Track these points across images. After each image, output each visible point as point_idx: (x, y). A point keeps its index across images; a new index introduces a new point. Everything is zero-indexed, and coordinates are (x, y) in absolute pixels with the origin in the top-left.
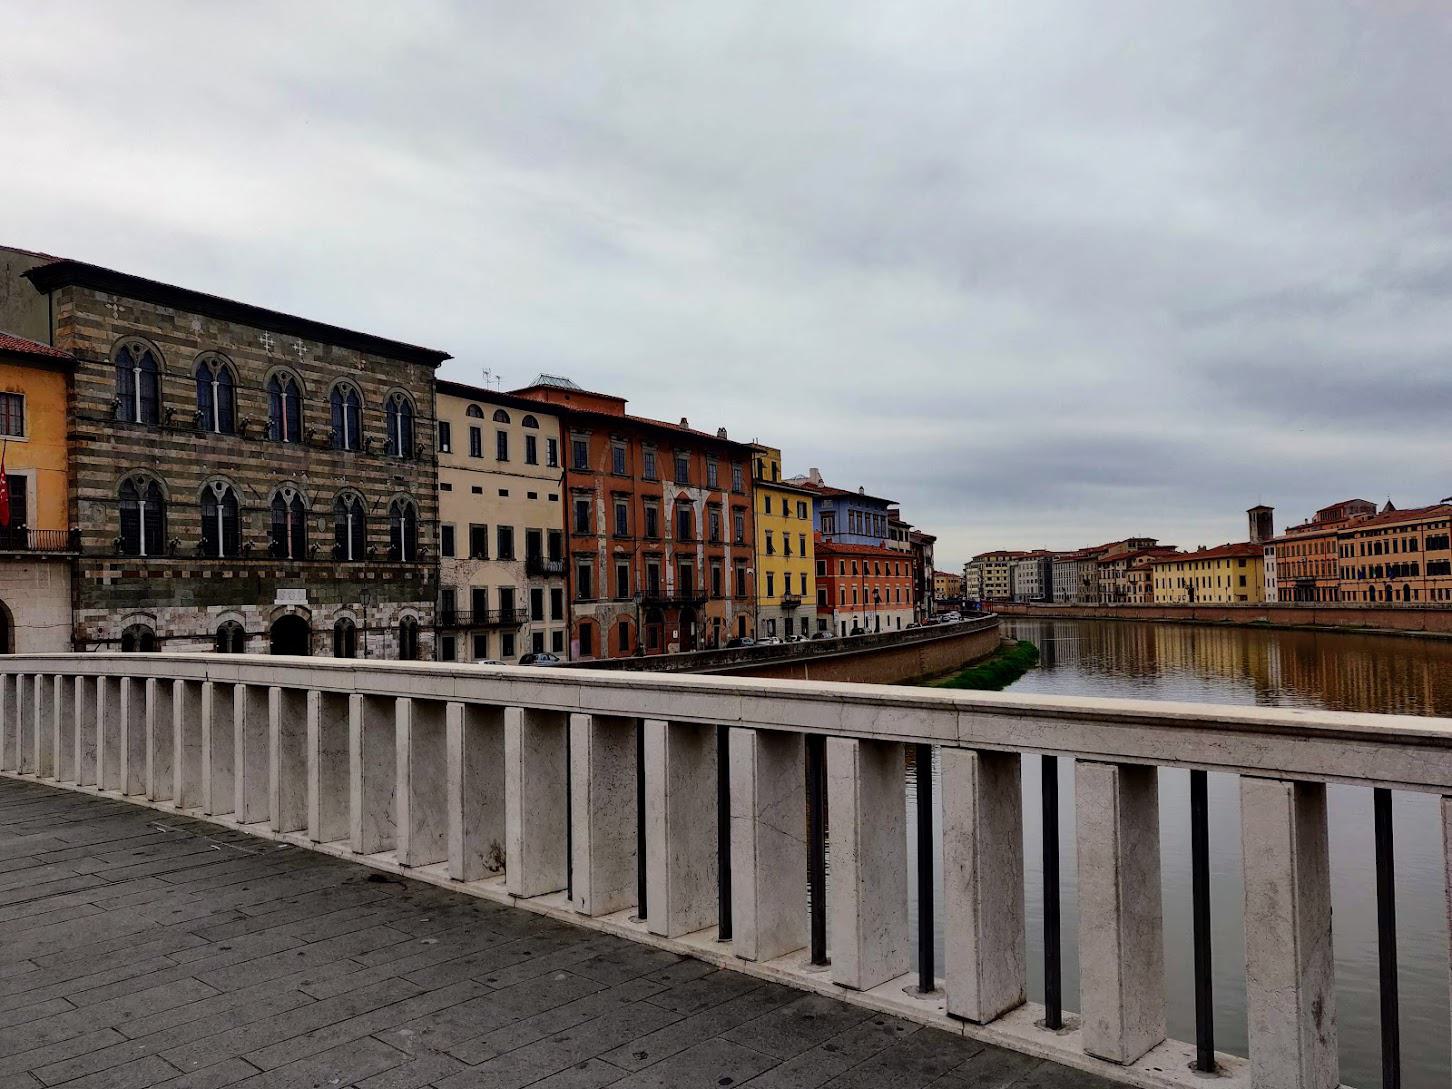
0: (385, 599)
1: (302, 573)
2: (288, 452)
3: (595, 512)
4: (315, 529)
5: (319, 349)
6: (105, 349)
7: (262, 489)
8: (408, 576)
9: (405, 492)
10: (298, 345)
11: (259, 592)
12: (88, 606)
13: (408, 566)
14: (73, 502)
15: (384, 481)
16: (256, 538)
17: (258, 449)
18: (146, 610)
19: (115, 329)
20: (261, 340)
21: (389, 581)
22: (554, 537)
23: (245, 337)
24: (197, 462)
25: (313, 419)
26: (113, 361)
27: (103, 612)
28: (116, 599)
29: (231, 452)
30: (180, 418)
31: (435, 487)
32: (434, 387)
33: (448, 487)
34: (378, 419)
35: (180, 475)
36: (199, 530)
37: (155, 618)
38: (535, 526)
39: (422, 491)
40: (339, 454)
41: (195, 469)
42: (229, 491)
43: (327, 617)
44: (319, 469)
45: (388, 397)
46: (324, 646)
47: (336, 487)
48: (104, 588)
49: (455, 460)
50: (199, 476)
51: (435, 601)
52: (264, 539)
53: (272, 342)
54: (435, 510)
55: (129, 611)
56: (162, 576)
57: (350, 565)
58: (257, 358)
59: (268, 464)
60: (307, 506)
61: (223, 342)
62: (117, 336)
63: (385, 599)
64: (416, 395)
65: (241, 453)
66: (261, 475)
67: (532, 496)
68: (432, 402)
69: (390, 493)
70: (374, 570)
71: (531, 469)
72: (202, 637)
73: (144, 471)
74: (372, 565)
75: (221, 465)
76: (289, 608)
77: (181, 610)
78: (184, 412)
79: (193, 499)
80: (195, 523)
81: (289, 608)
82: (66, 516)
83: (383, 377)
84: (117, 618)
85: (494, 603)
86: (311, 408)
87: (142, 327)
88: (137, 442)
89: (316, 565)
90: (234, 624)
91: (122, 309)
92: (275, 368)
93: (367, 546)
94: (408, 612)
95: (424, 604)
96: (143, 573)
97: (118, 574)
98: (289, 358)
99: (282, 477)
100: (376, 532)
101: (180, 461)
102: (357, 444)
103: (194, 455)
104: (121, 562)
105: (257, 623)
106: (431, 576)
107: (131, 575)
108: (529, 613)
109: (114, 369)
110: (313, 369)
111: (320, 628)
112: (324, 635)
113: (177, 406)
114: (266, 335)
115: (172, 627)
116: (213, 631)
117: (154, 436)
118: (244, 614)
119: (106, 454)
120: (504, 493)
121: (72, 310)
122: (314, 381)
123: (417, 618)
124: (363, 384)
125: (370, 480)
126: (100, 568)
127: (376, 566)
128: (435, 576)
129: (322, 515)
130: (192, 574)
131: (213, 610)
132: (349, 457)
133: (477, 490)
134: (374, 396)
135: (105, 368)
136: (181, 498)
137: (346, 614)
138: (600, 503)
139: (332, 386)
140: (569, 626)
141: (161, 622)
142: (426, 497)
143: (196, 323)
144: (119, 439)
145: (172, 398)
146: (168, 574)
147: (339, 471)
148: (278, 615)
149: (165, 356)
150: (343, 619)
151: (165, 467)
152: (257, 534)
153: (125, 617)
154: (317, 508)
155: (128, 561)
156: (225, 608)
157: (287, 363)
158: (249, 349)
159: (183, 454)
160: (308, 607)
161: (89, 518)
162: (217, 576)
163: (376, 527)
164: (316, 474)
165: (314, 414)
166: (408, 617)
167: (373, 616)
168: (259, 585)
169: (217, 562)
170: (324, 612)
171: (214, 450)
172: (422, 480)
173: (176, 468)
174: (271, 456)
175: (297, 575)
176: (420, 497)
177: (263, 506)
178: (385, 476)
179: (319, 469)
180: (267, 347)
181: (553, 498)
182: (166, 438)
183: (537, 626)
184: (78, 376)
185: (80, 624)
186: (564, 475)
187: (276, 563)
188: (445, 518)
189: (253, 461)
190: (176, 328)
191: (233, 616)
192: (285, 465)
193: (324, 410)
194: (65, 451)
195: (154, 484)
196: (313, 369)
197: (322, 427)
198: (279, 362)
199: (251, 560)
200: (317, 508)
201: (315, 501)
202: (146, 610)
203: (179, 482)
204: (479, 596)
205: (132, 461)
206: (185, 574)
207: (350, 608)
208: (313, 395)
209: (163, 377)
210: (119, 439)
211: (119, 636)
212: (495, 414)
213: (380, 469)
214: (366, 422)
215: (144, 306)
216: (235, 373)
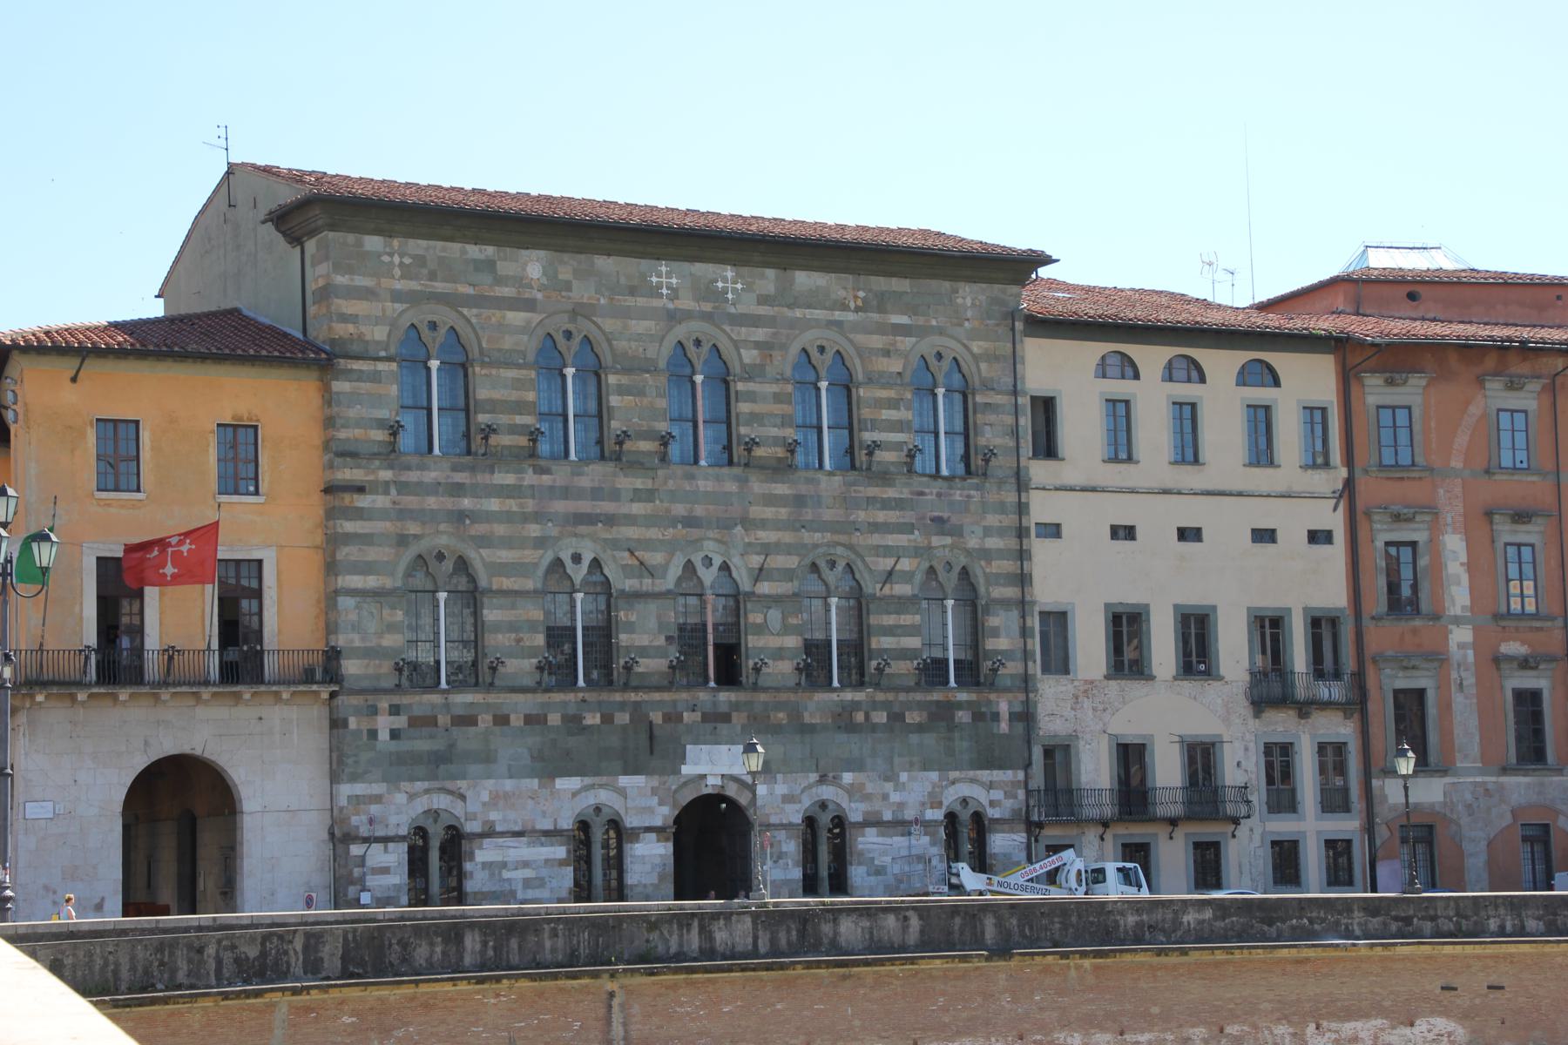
0: (912, 764)
1: (734, 715)
2: (704, 485)
3: (1437, 566)
4: (761, 629)
5: (769, 279)
6: (379, 333)
7: (655, 558)
8: (963, 716)
9: (952, 547)
10: (725, 280)
11: (652, 753)
12: (354, 778)
13: (963, 696)
14: (331, 598)
15: (907, 528)
16: (644, 651)
17: (649, 484)
18: (449, 785)
19: (397, 296)
20: (654, 279)
21: (920, 728)
22: (1319, 624)
23: (623, 280)
24: (538, 517)
25: (755, 418)
26: (393, 351)
27: (378, 788)
28: (401, 766)
29: (596, 494)
30: (505, 440)
31: (1022, 532)
32: (1019, 325)
33: (1053, 531)
34: (893, 404)
35: (508, 543)
36: (540, 640)
37: (463, 797)
38: (1270, 602)
39: (993, 543)
40: (809, 481)
41: (534, 530)
42: (596, 564)
43: (788, 799)
44: (769, 513)
45: (915, 360)
46: (780, 856)
47: (804, 546)
48: (379, 746)
50: (541, 543)
51: (1028, 766)
52: (659, 652)
53: (674, 281)
54: (1023, 580)
55: (420, 786)
56: (476, 724)
57: (834, 696)
58: (644, 314)
59: (668, 510)
60: (746, 586)
61: (583, 292)
62: (399, 307)
63: (912, 764)
64: (977, 347)
65: (615, 495)
66: (653, 533)
67: (1264, 536)
68: (1015, 359)
69: (917, 552)
70: (886, 705)
72: (546, 833)
73: (443, 541)
74: (880, 696)
76: (711, 781)
77: (509, 785)
78: (514, 429)
79: (530, 585)
80: (532, 626)
81: (711, 781)
82: (322, 624)
83: (903, 319)
84: (400, 798)
85: (1167, 772)
86: (751, 397)
87: (440, 286)
88: (434, 488)
89: (763, 697)
90: (605, 810)
91: (407, 261)
92: (680, 332)
93: (870, 659)
94: (965, 790)
95: (1007, 775)
96: (443, 720)
97: (401, 722)
98: (707, 307)
99: (695, 533)
100: (890, 631)
101: (507, 517)
102: (854, 458)
103: (530, 505)
104: (405, 700)
105: (650, 810)
106: (1013, 717)
107: (423, 722)
108: (1258, 797)
109: (394, 366)
110: (754, 321)
111: (774, 820)
112: (782, 835)
113: (504, 419)
114: (664, 269)
115: (494, 816)
116: (567, 823)
117: (460, 477)
118: (622, 792)
119: (383, 515)
120: (1188, 534)
121: (328, 275)
122: (757, 345)
123: (985, 803)
124: (860, 338)
125: (875, 527)
126: (373, 711)
127: (890, 696)
128: (1026, 717)
129: (776, 600)
130: (529, 720)
131: (566, 784)
132: (831, 485)
133: (1123, 533)
134: (885, 360)
135: (381, 366)
136: (507, 583)
137: (827, 792)
138: (1454, 545)
139: (795, 349)
140: (1369, 828)
141: (473, 806)
142: (1001, 554)
143: (533, 265)
144: (403, 487)
145: (493, 406)
146: (485, 720)
147: (808, 514)
148: (687, 796)
149: (480, 332)
150: (823, 805)
151: (480, 529)
152: (646, 643)
153: (412, 797)
154: (765, 588)
155: (417, 698)
156: (588, 780)
157: (707, 317)
158: (630, 301)
159: (512, 505)
161: (356, 627)
162: (573, 722)
163: (889, 620)
164: (763, 524)
165: (758, 408)
166: (965, 801)
167: (885, 797)
168: (651, 737)
169: (570, 697)
170: (781, 789)
171: (566, 493)
172: (992, 520)
173: (500, 530)
174: (674, 497)
176: (986, 554)
177: (657, 589)
178: (909, 516)
179: (769, 513)
180: (665, 291)
181: (1318, 537)
182: (483, 478)
183: (1283, 826)
184: (339, 386)
185: (341, 809)
186: (1349, 483)
187: (684, 695)
188: (1046, 594)
189: (637, 508)
190: (500, 281)
191: (604, 797)
192: (699, 511)
193: (778, 398)
194: (321, 512)
195: (462, 565)
196: (754, 321)
197: (774, 432)
198: (688, 315)
199: (636, 689)
200: (765, 588)
201: (760, 574)
202: (449, 785)
203: (505, 555)
204: (1131, 756)
205: (424, 523)
206: (516, 721)
207: (836, 781)
208: (751, 374)
209: (477, 369)
210: (403, 487)
211: (403, 831)
212: (1170, 366)
213: (899, 504)
214: (866, 413)
215: (444, 249)
216: (605, 345)
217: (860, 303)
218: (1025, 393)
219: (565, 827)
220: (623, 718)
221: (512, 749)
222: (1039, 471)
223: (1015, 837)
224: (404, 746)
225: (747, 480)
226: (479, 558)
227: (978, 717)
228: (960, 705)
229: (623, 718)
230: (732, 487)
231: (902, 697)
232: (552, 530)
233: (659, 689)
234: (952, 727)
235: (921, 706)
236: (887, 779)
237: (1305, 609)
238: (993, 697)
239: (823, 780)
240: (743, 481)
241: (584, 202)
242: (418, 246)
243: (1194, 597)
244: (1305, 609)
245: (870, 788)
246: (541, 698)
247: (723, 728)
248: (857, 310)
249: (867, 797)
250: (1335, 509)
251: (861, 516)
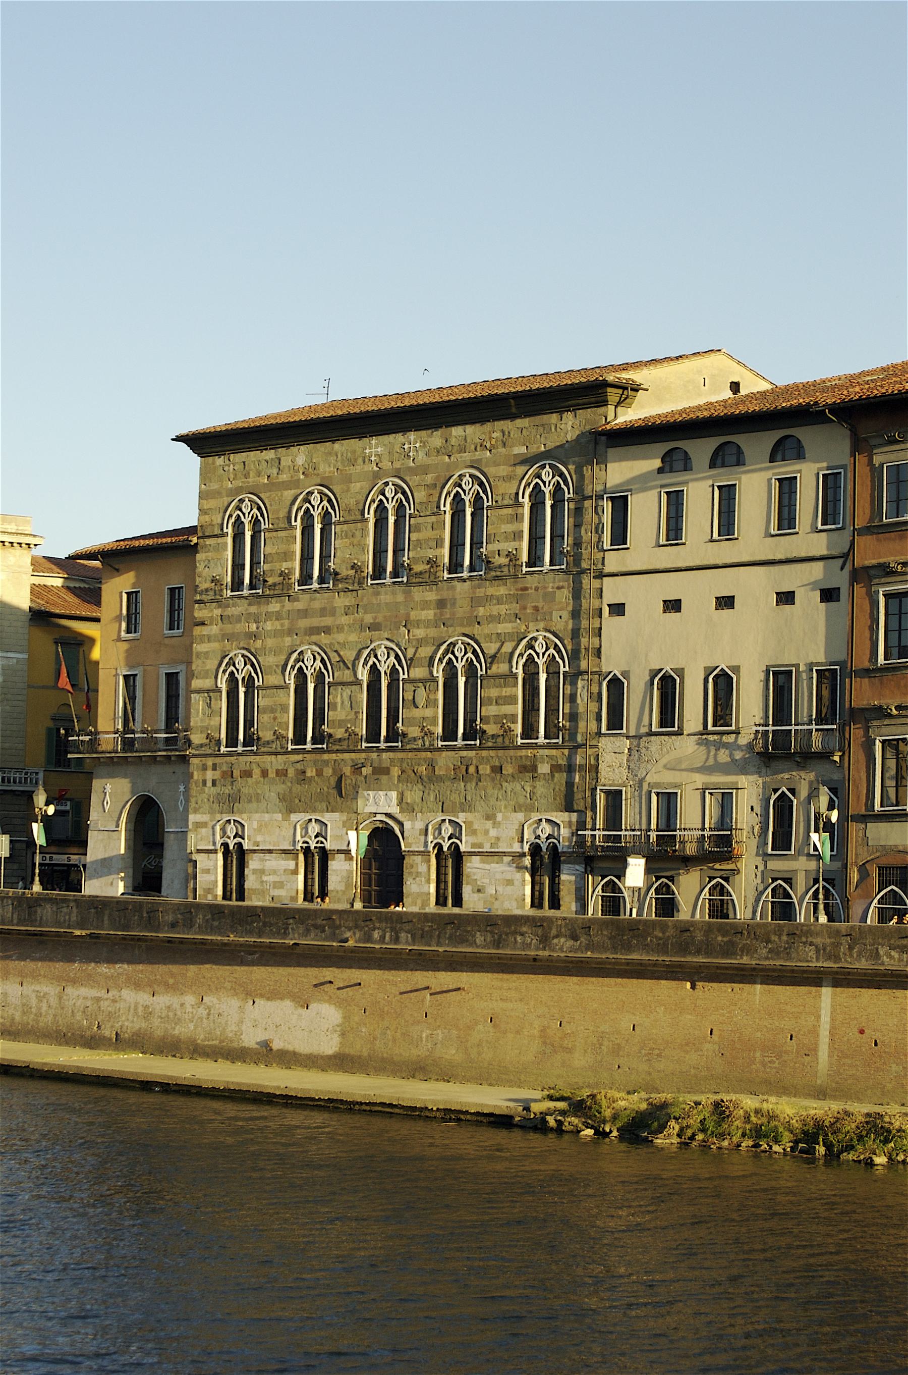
5: (436, 438)
29: (323, 612)
33: (618, 609)
38: (787, 658)
61: (326, 469)
71: (726, 552)
115: (259, 838)
126: (204, 768)
130: (278, 772)
133: (673, 606)
146: (257, 772)
160: (400, 817)
163: (494, 692)
167: (487, 832)
171: (305, 613)
175: (386, 771)
217: (493, 442)
220: (328, 771)
221: (272, 791)
222: (613, 561)
223: (577, 867)
225: (410, 592)
229: (328, 771)
236: (488, 817)
240: (408, 594)
241: (293, 412)
247: (384, 778)
250: (842, 569)
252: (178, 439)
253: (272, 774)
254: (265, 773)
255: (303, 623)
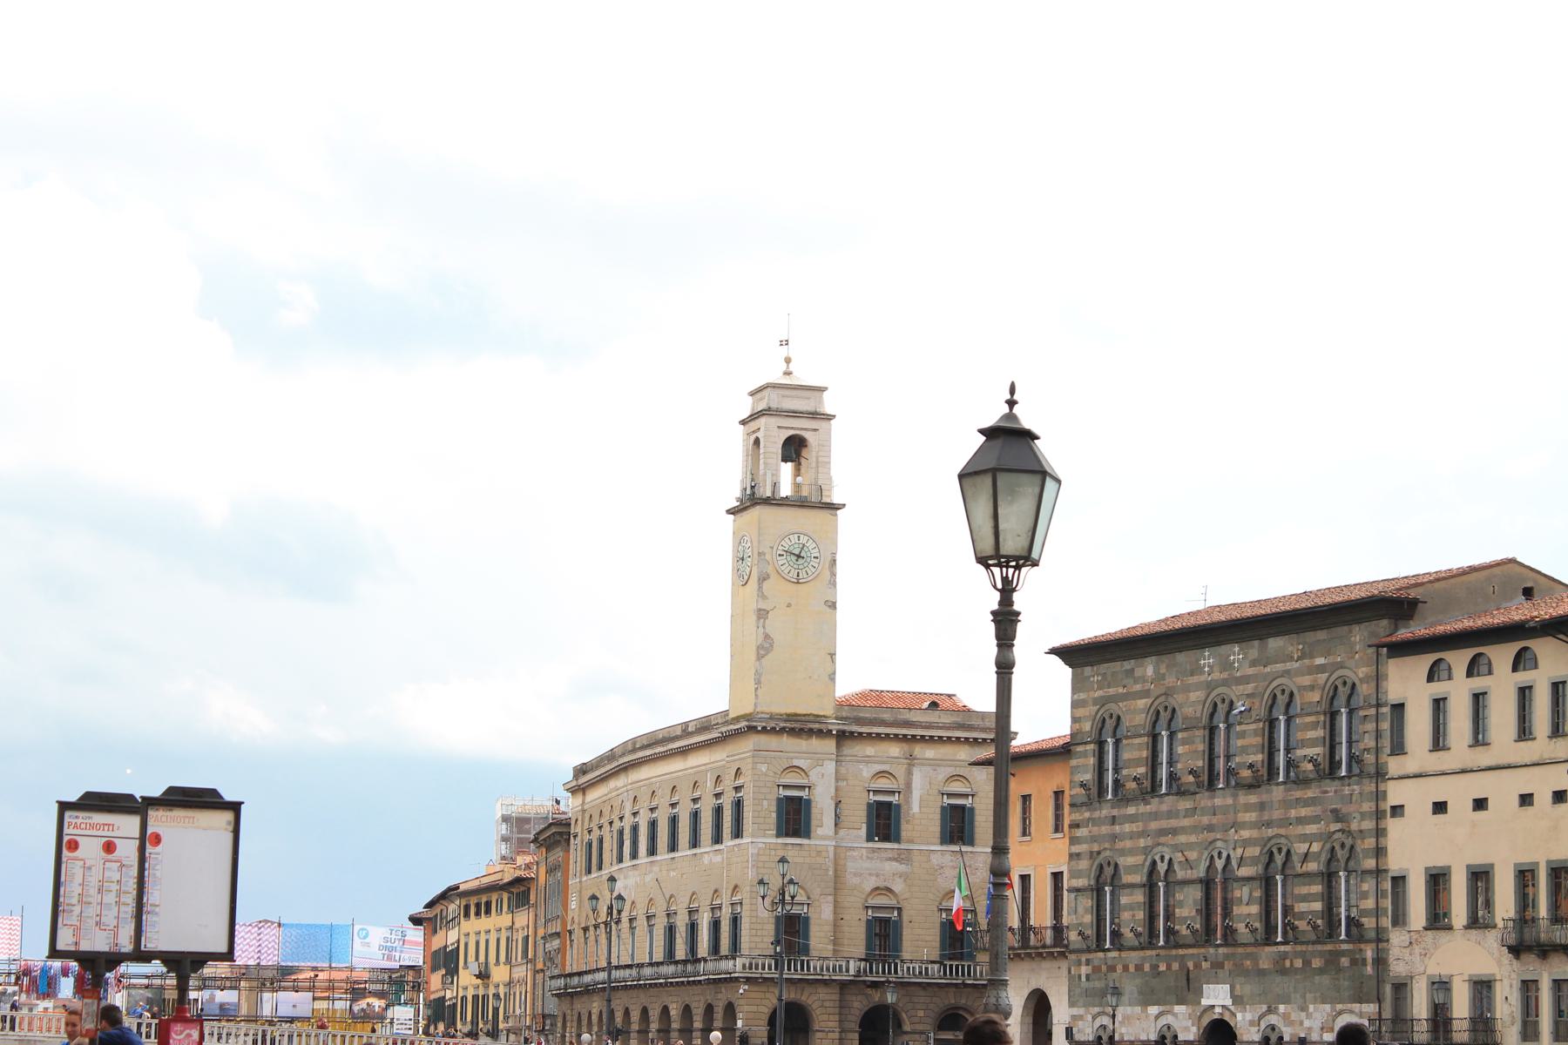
5: (1254, 650)
7: (1192, 855)
8: (1345, 962)
15: (1315, 819)
21: (1321, 971)
24: (1143, 834)
33: (1397, 810)
41: (1142, 842)
43: (1252, 1023)
49: (1410, 764)
54: (1380, 852)
55: (1097, 1010)
58: (1197, 687)
66: (1193, 839)
74: (1299, 948)
75: (1163, 832)
76: (1218, 1010)
85: (1461, 1007)
89: (1240, 950)
99: (1212, 836)
105: (1187, 1029)
115: (1123, 1030)
120: (1480, 804)
125: (1301, 821)
126: (1079, 963)
127: (1304, 948)
128: (1381, 962)
131: (1153, 1010)
137: (1273, 1019)
146: (1119, 968)
148: (1206, 1021)
156: (1162, 1008)
167: (1301, 1023)
169: (1154, 952)
170: (1249, 1016)
174: (1204, 811)
188: (1395, 864)
189: (1186, 822)
218: (1385, 704)
219: (1191, 1037)
220: (1175, 966)
222: (1394, 765)
224: (1091, 985)
226: (1122, 861)
227: (1354, 962)
228: (1343, 953)
229: (1175, 966)
230: (1230, 801)
231: (1310, 948)
232: (1149, 841)
233: (1190, 946)
234: (1339, 970)
235: (1321, 954)
237: (1548, 862)
238: (1362, 946)
239: (1270, 1011)
240: (1235, 796)
241: (1141, 627)
242: (1104, 667)
243: (1478, 859)
244: (1548, 862)
245: (1293, 1017)
246: (1141, 953)
248: (1299, 659)
249: (1290, 1023)
251: (1293, 813)
252: (1054, 651)
253: (1132, 969)
254: (1126, 968)
255: (1154, 825)
